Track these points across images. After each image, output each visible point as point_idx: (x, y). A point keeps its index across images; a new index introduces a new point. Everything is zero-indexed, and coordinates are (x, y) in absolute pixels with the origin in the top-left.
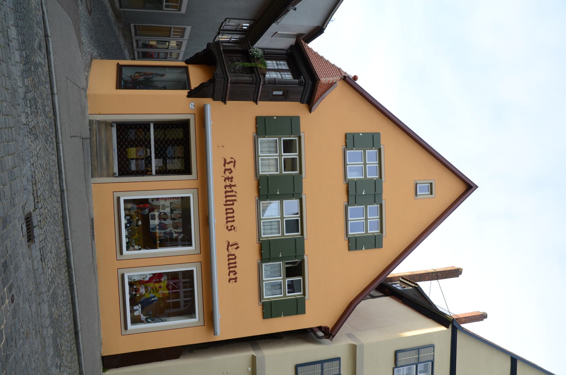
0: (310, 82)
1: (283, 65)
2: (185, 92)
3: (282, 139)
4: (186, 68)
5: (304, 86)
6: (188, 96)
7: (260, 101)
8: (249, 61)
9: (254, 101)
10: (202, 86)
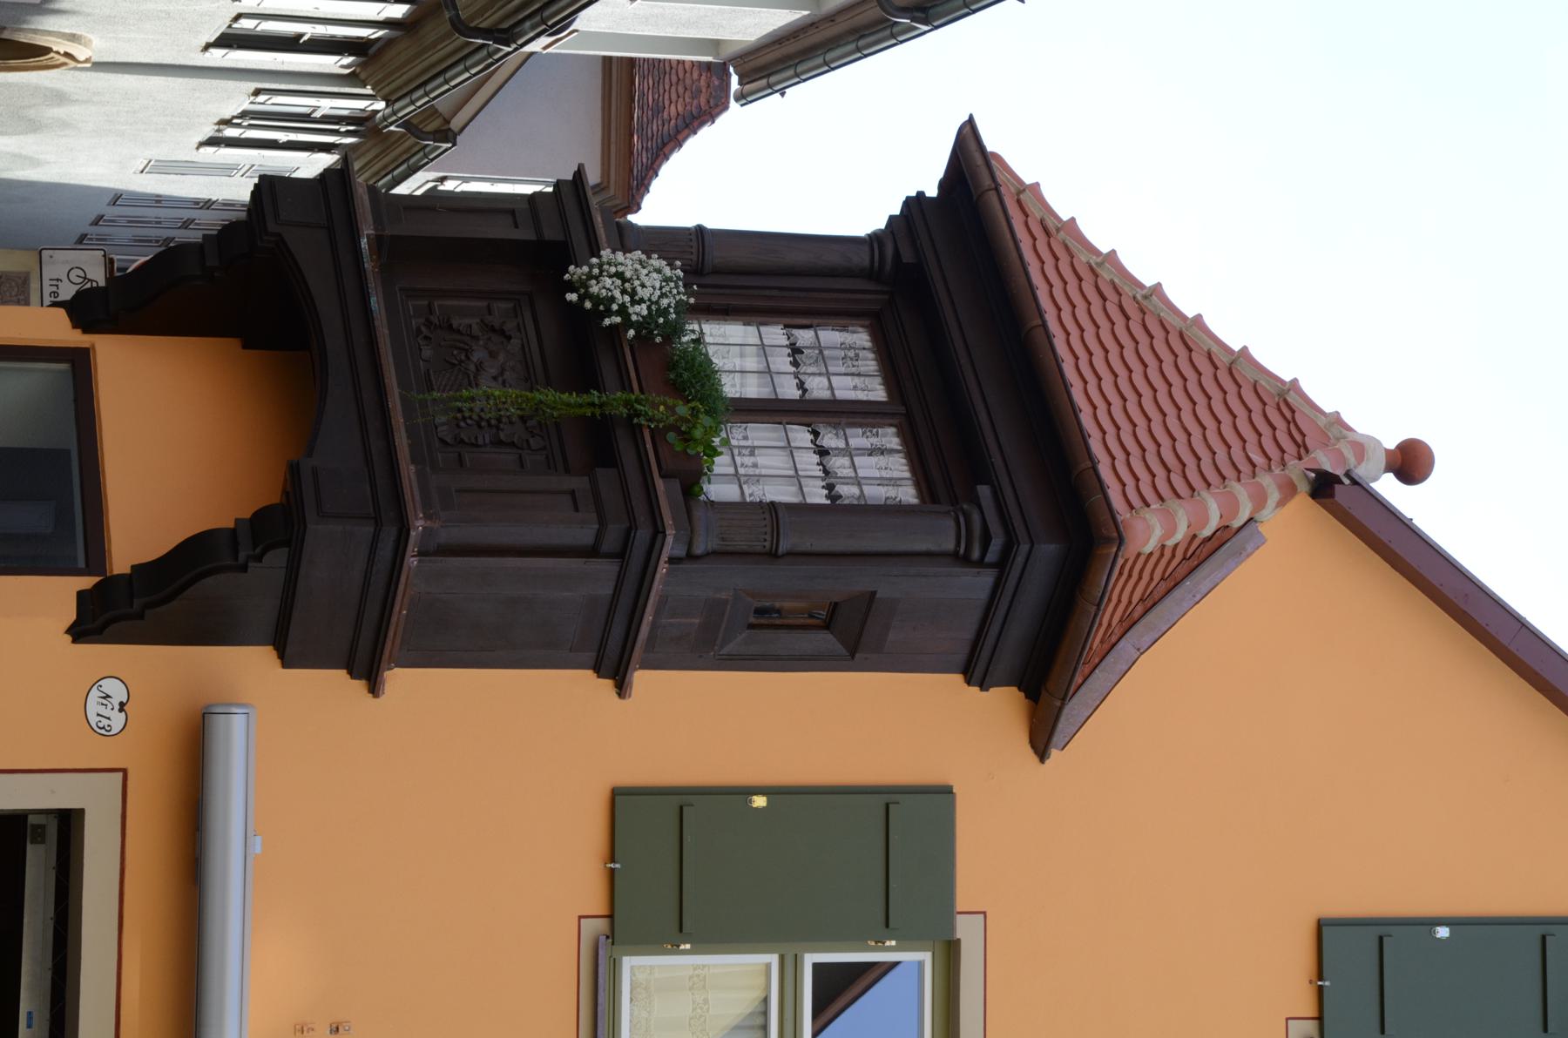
0: (1048, 551)
1: (847, 364)
2: (59, 595)
3: (810, 959)
4: (80, 361)
5: (1002, 565)
6: (81, 632)
7: (646, 665)
8: (585, 379)
9: (599, 670)
10: (193, 559)
